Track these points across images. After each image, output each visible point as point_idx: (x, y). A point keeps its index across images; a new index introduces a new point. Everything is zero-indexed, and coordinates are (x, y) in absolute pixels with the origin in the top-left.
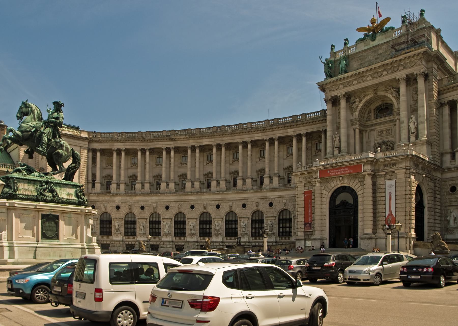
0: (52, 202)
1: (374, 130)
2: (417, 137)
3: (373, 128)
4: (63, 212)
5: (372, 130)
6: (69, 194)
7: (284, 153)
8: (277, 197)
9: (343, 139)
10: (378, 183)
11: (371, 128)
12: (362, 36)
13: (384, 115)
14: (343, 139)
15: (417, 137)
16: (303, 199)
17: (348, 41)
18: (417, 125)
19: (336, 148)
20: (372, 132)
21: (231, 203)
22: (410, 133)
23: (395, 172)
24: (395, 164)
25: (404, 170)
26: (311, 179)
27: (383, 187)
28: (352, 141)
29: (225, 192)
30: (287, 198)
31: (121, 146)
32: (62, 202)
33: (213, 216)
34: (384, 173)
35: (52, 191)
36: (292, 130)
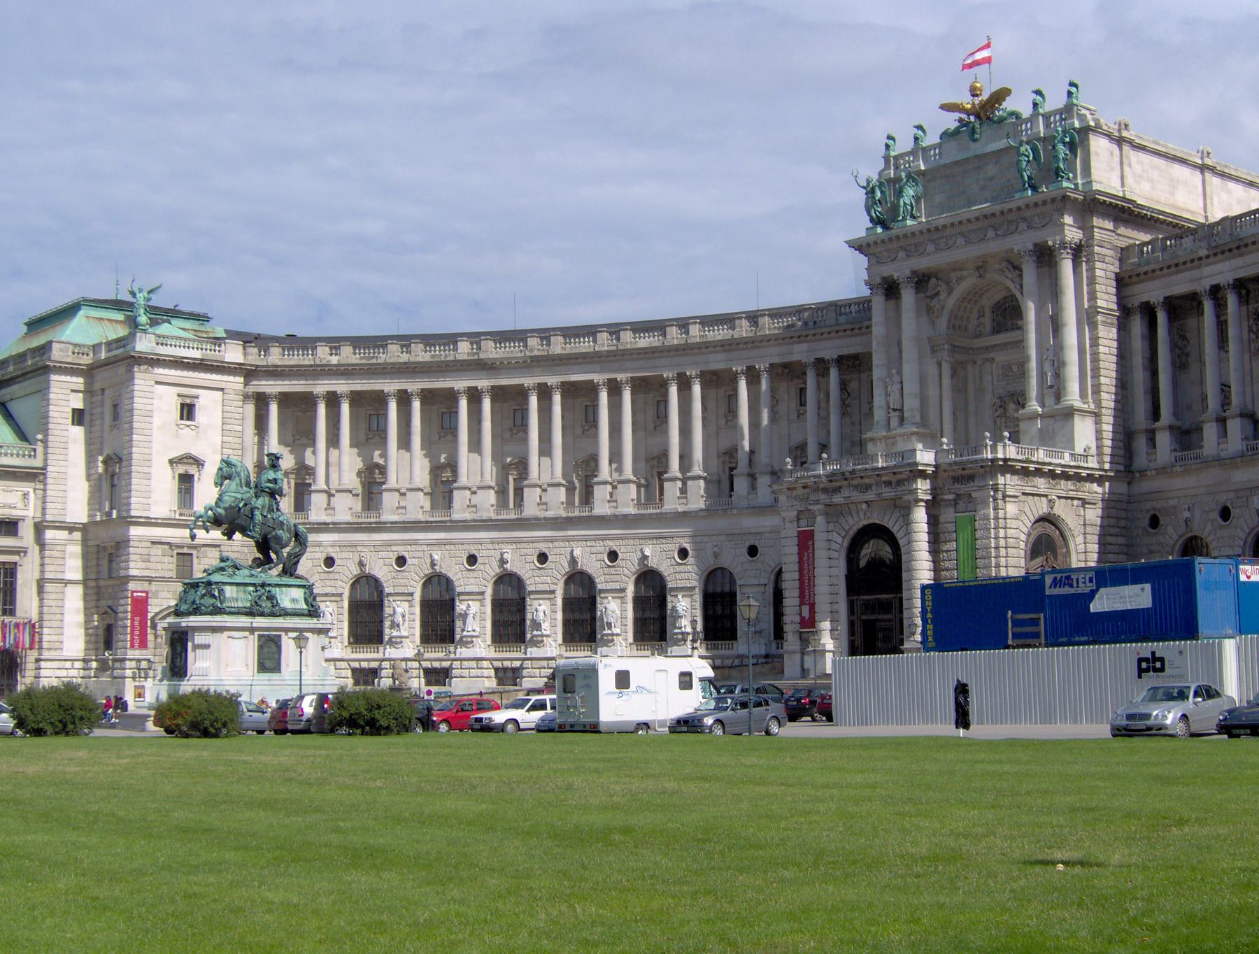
0: (273, 615)
3: (991, 355)
4: (287, 630)
6: (294, 601)
7: (788, 403)
9: (911, 387)
10: (942, 519)
11: (985, 356)
12: (953, 125)
14: (911, 387)
17: (924, 131)
19: (894, 410)
23: (974, 495)
24: (971, 478)
28: (933, 392)
31: (342, 386)
32: (286, 613)
34: (951, 497)
35: (271, 598)
36: (804, 347)
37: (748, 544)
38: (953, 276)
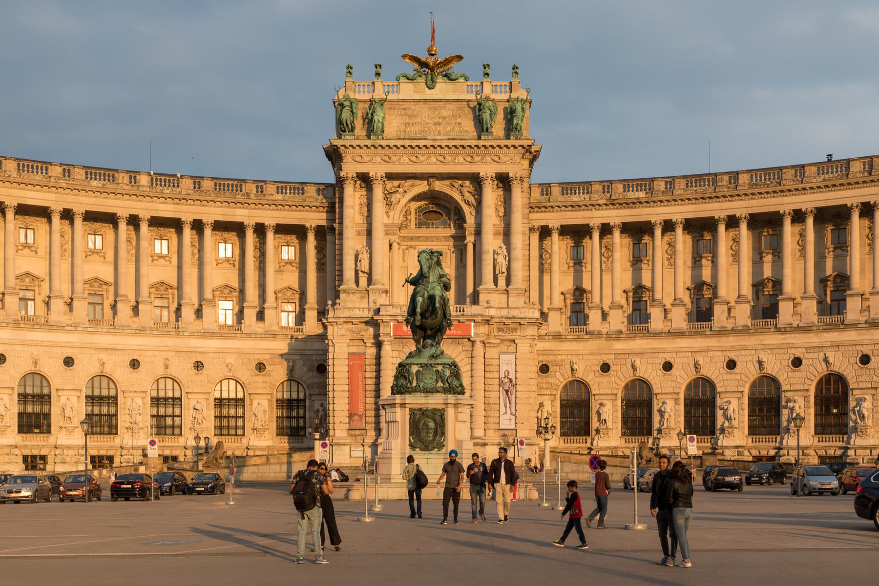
1: (414, 247)
2: (508, 282)
3: (413, 243)
8: (213, 350)
11: (409, 244)
13: (433, 224)
15: (508, 282)
16: (346, 368)
18: (509, 261)
20: (411, 250)
21: (103, 356)
22: (497, 272)
24: (515, 330)
25: (530, 341)
26: (364, 333)
27: (496, 362)
29: (89, 329)
30: (236, 356)
33: (55, 383)
34: (498, 341)
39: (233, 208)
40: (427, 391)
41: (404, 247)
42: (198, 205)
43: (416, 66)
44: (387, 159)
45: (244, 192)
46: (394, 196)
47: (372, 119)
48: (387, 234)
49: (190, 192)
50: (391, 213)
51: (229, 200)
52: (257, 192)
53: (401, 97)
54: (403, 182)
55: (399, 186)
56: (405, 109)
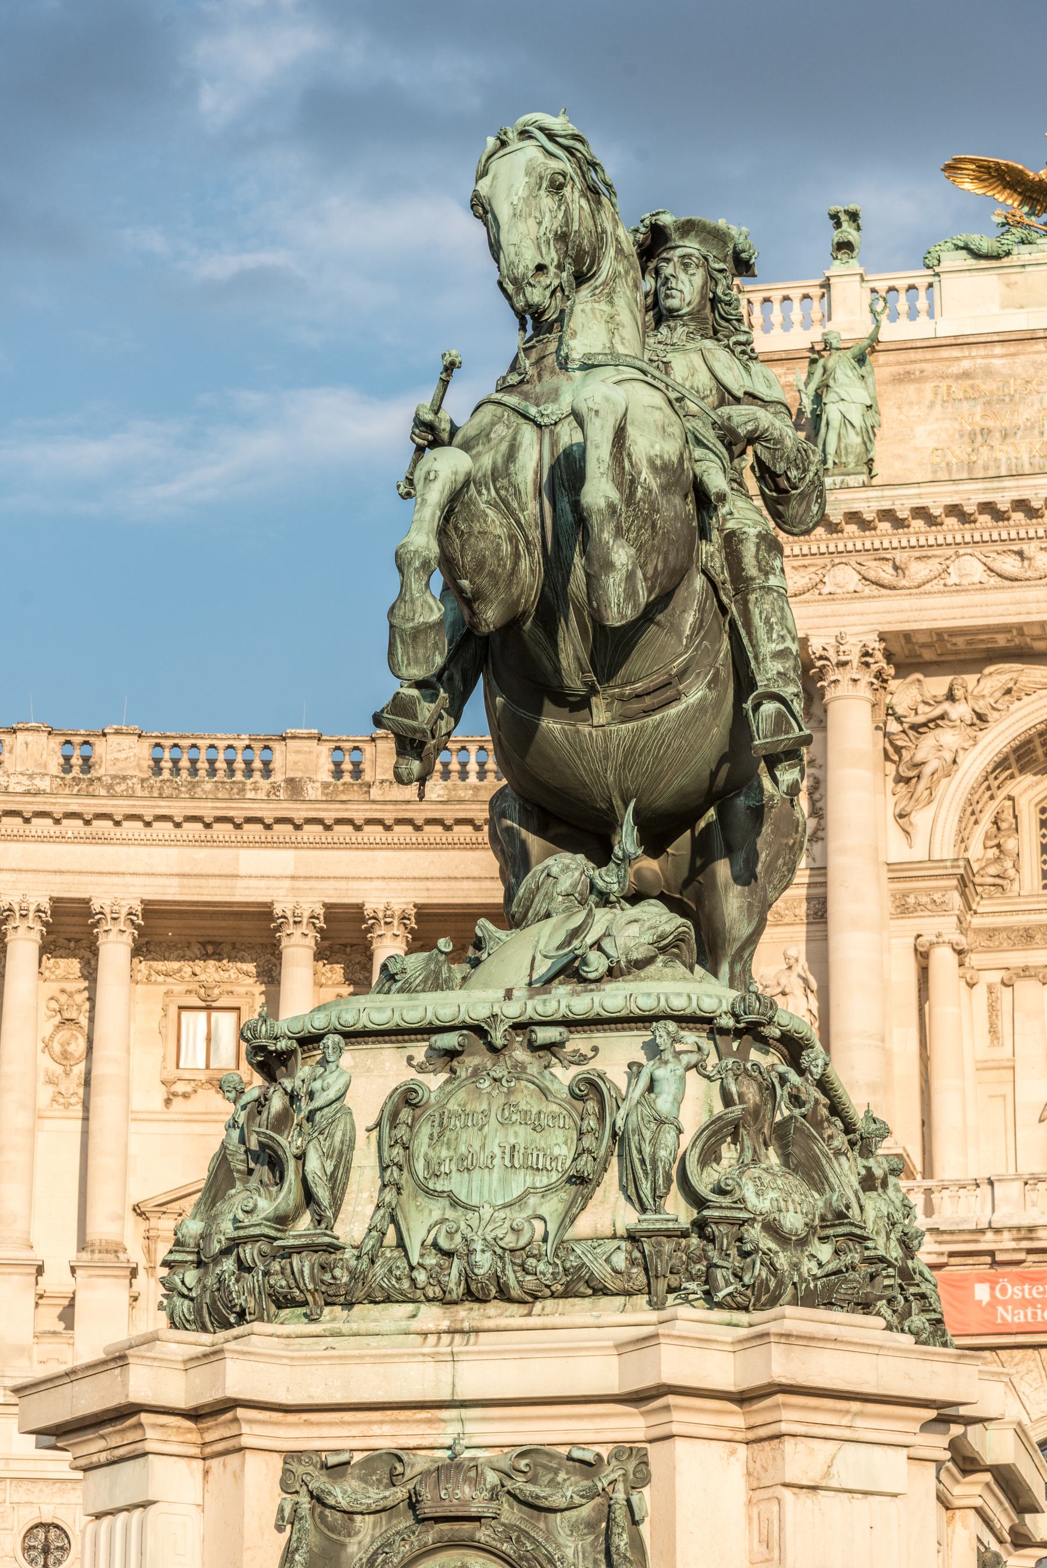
5: (1025, 972)
11: (1017, 958)
36: (279, 861)
37: (29, 1517)
38: (998, 676)
39: (227, 844)
40: (483, 1286)
41: (995, 977)
42: (77, 840)
43: (1008, 201)
44: (886, 573)
45: (278, 777)
46: (929, 741)
47: (817, 417)
48: (903, 909)
49: (44, 784)
50: (921, 819)
51: (208, 810)
52: (338, 773)
53: (946, 327)
54: (971, 679)
55: (951, 697)
56: (966, 375)
